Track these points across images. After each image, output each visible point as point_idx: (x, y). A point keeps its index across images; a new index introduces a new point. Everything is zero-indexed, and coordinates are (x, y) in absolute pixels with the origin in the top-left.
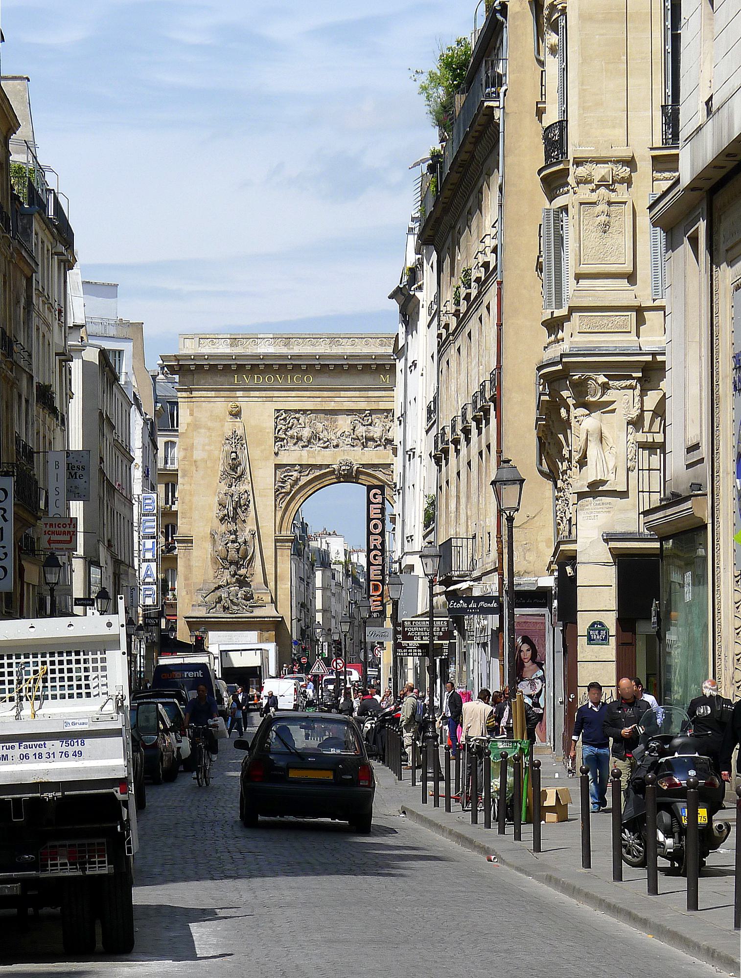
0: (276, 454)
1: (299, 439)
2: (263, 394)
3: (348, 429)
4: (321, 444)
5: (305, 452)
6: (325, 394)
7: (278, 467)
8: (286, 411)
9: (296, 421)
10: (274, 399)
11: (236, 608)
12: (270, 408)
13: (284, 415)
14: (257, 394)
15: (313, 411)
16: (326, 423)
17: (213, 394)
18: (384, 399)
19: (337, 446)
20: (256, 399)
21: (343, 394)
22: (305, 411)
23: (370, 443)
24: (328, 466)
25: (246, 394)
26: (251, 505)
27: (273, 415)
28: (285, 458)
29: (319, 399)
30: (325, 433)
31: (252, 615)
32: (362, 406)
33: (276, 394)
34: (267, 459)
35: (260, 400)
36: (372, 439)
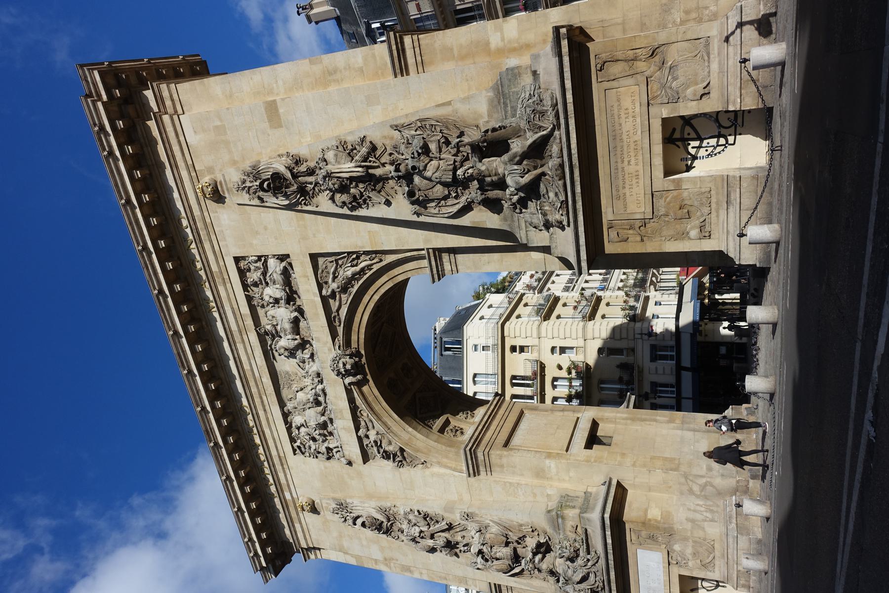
0: (350, 463)
1: (324, 426)
2: (279, 467)
3: (293, 361)
4: (321, 399)
5: (338, 423)
6: (254, 390)
7: (366, 458)
8: (292, 440)
9: (303, 429)
10: (282, 455)
11: (592, 576)
12: (296, 462)
13: (298, 443)
14: (281, 475)
15: (282, 404)
16: (295, 387)
17: (297, 526)
18: (235, 306)
19: (318, 375)
20: (289, 476)
21: (246, 367)
22: (286, 415)
23: (302, 324)
24: (349, 392)
25: (285, 488)
26: (424, 509)
27: (300, 457)
28: (353, 450)
29: (264, 398)
30: (306, 390)
31: (602, 556)
32: (253, 337)
33: (274, 453)
34: (360, 475)
35: (287, 471)
36: (296, 322)
